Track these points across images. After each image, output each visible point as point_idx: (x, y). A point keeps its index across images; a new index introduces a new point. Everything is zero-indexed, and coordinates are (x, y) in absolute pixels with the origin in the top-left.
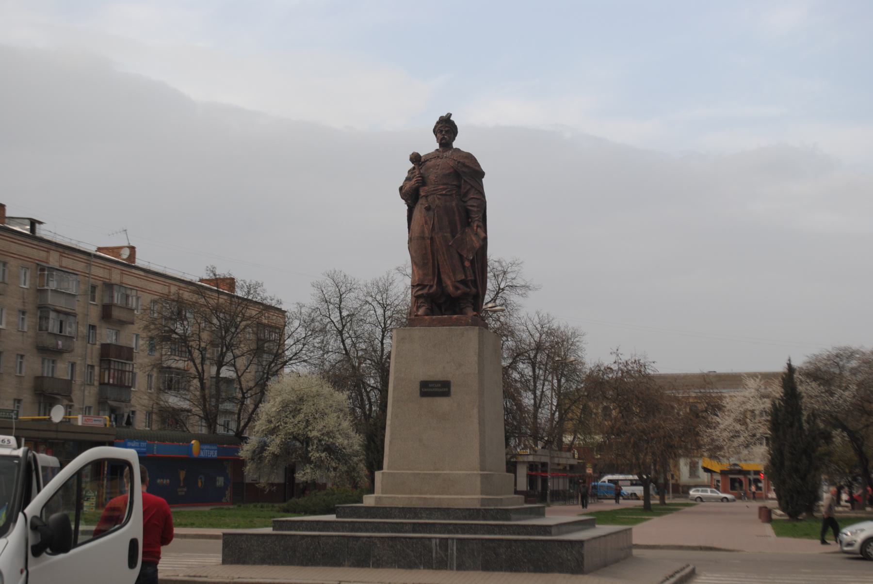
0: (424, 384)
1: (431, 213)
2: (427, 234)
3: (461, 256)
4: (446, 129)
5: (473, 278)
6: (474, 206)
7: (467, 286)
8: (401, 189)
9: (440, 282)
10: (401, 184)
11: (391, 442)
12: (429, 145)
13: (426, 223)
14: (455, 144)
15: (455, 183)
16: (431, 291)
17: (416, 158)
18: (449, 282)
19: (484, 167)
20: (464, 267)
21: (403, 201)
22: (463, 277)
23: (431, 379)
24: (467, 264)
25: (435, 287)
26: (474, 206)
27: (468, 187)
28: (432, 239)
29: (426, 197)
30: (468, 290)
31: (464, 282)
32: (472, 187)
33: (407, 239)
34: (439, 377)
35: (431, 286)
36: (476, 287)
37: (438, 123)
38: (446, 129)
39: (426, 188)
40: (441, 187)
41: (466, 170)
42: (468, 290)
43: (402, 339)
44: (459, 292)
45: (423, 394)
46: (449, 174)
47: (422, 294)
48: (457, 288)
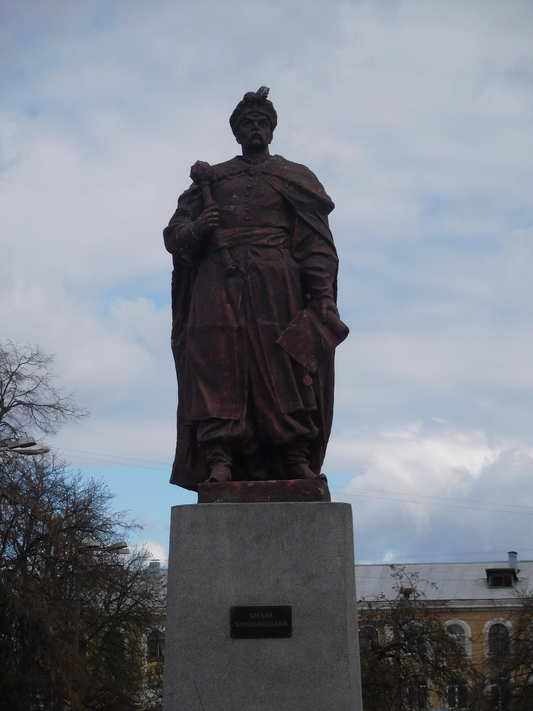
4: (254, 117)
5: (316, 407)
7: (306, 424)
8: (168, 233)
10: (166, 225)
12: (224, 148)
14: (273, 149)
15: (283, 224)
16: (236, 432)
19: (331, 191)
20: (301, 385)
22: (302, 406)
23: (254, 604)
24: (308, 380)
30: (306, 430)
34: (268, 600)
36: (319, 424)
38: (254, 117)
39: (228, 232)
42: (306, 430)
45: (238, 633)
47: (220, 438)
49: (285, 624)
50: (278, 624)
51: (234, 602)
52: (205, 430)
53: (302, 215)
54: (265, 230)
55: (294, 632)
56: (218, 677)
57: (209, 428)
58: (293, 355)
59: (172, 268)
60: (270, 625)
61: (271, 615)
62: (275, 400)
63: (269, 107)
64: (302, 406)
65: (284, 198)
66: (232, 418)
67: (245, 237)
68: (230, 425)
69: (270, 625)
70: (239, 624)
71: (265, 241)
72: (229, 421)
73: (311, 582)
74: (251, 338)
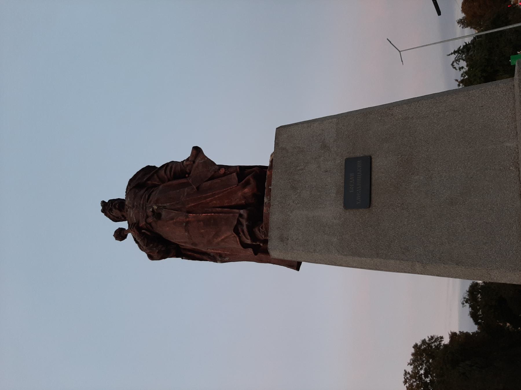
1: (164, 213)
3: (212, 178)
6: (171, 168)
8: (151, 257)
9: (239, 207)
13: (172, 219)
17: (120, 235)
18: (240, 194)
22: (235, 174)
23: (342, 189)
25: (242, 211)
26: (171, 168)
27: (155, 176)
28: (189, 212)
33: (212, 263)
34: (339, 178)
35: (241, 215)
37: (106, 215)
43: (282, 240)
44: (252, 181)
45: (368, 203)
47: (248, 226)
48: (247, 183)
55: (367, 154)
56: (406, 220)
57: (242, 233)
59: (180, 259)
62: (229, 190)
63: (112, 201)
64: (235, 174)
65: (134, 187)
67: (143, 208)
68: (241, 219)
71: (147, 196)
74: (193, 204)
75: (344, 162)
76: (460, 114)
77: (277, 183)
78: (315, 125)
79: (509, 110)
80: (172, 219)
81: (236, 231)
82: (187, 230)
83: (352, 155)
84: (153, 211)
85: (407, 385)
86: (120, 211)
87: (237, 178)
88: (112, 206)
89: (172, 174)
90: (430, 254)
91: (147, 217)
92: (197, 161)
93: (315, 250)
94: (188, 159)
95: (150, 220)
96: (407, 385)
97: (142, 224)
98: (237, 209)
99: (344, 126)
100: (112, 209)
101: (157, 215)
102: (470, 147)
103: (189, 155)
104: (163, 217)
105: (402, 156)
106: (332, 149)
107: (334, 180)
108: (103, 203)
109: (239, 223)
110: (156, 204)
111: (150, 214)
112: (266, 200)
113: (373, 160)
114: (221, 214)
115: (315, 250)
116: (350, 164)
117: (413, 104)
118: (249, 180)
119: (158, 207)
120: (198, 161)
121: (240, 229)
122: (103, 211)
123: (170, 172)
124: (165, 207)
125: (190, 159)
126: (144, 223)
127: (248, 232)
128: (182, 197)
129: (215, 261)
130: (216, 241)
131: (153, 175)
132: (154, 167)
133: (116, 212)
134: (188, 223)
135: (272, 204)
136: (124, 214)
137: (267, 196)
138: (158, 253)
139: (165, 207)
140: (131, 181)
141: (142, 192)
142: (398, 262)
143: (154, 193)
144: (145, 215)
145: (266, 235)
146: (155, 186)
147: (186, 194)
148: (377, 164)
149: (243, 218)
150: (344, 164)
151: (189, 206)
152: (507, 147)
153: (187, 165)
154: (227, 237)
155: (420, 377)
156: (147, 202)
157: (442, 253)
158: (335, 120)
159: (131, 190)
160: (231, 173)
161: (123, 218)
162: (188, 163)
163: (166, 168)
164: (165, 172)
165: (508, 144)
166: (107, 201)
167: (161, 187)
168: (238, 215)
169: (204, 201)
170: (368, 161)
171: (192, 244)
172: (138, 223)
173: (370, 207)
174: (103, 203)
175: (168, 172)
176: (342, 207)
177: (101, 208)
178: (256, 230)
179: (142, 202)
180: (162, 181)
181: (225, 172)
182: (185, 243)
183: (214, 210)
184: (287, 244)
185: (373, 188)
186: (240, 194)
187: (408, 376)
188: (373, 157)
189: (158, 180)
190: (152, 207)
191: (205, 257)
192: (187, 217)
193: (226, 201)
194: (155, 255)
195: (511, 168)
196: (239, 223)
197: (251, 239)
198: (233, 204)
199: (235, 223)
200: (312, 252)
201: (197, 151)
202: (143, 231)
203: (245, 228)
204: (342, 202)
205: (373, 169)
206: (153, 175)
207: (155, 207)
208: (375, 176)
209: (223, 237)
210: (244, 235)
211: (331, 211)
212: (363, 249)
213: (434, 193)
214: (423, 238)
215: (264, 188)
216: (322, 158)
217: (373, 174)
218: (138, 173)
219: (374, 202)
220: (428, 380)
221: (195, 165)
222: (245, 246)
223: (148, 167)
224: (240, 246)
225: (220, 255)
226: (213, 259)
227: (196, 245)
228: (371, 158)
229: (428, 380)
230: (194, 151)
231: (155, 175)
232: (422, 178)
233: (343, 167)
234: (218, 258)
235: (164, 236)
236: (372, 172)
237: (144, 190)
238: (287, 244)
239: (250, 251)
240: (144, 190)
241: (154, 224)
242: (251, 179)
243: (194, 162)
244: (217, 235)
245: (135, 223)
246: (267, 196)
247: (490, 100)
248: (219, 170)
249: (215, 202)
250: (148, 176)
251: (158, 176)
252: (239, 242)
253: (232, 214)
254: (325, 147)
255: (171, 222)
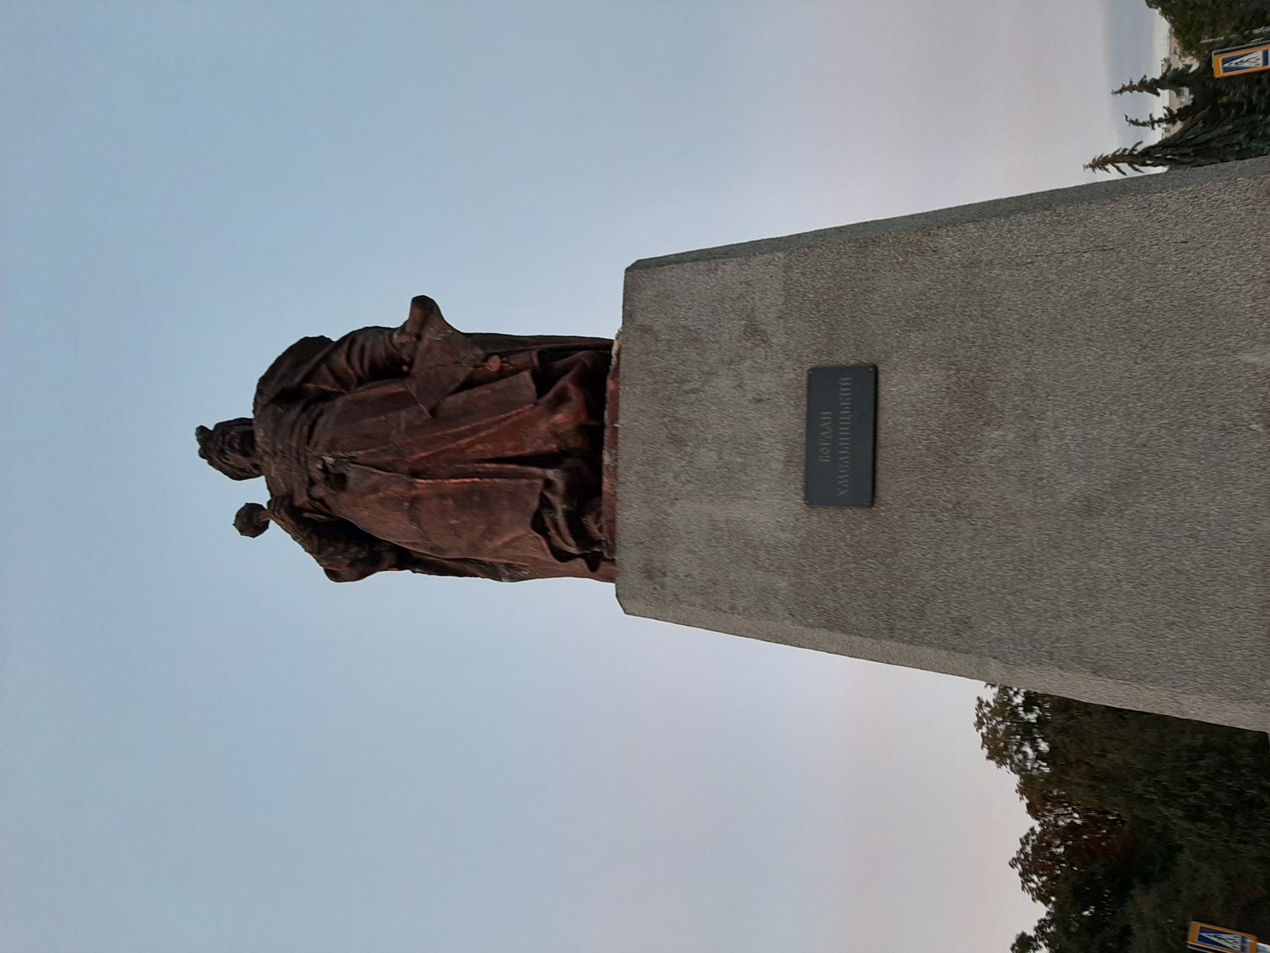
0: (817, 491)
1: (352, 474)
2: (398, 489)
3: (469, 384)
6: (362, 349)
8: (334, 575)
11: (1097, 670)
13: (375, 490)
16: (560, 485)
18: (543, 426)
20: (502, 374)
21: (379, 576)
22: (526, 374)
23: (801, 452)
24: (494, 364)
25: (550, 473)
26: (362, 349)
28: (415, 474)
29: (312, 483)
31: (543, 380)
32: (327, 358)
35: (548, 484)
37: (211, 463)
40: (295, 437)
41: (279, 374)
44: (573, 391)
46: (277, 420)
47: (568, 515)
48: (561, 399)
49: (845, 381)
50: (845, 397)
51: (796, 501)
52: (558, 538)
53: (298, 379)
54: (297, 429)
55: (865, 358)
56: (967, 546)
58: (453, 387)
59: (409, 572)
60: (846, 415)
61: (826, 415)
62: (516, 418)
63: (223, 427)
65: (272, 401)
66: (538, 491)
69: (846, 415)
70: (844, 488)
72: (543, 498)
73: (763, 327)
74: (423, 454)
75: (805, 377)
76: (1122, 262)
77: (633, 412)
78: (728, 268)
79: (1258, 259)
80: (375, 490)
81: (539, 525)
82: (415, 519)
83: (826, 361)
84: (325, 469)
85: (984, 730)
86: (246, 454)
87: (533, 386)
88: (223, 442)
89: (366, 364)
90: (1026, 641)
91: (312, 483)
92: (427, 336)
93: (733, 608)
94: (402, 329)
95: (319, 491)
96: (984, 730)
97: (301, 500)
98: (538, 466)
99: (804, 274)
100: (225, 446)
101: (338, 481)
102: (1145, 359)
103: (407, 318)
104: (351, 483)
105: (958, 371)
106: (774, 340)
107: (779, 425)
108: (202, 431)
109: (545, 503)
110: (329, 451)
111: (318, 476)
112: (607, 459)
113: (882, 377)
114: (497, 480)
115: (733, 608)
116: (821, 381)
117: (993, 223)
118: (564, 389)
119: (337, 458)
120: (430, 335)
121: (547, 520)
122: (204, 454)
123: (361, 360)
124: (352, 460)
125: (408, 329)
126: (306, 498)
127: (571, 527)
128: (394, 432)
129: (497, 576)
130: (490, 545)
131: (317, 367)
132: (322, 341)
133: (236, 459)
134: (415, 500)
135: (621, 479)
136: (258, 462)
137: (611, 447)
138: (350, 565)
139: (352, 460)
140: (263, 382)
141: (294, 413)
142: (944, 653)
143: (322, 420)
144: (306, 479)
145: (612, 535)
146: (326, 397)
147: (403, 426)
148: (893, 388)
149: (554, 493)
150: (804, 383)
151: (415, 457)
152: (1246, 364)
153: (403, 345)
154: (515, 539)
155: (1014, 713)
156: (308, 444)
157: (1058, 639)
158: (781, 255)
159: (264, 407)
160: (517, 371)
161: (256, 472)
162: (404, 339)
163: (350, 348)
164: (348, 359)
165: (1252, 359)
166: (211, 428)
167: (339, 403)
168: (540, 482)
169: (452, 446)
170: (869, 377)
171: (432, 549)
172: (290, 496)
173: (872, 504)
174: (202, 431)
175: (356, 363)
176: (799, 499)
177: (198, 446)
178: (589, 521)
179: (294, 444)
180: (343, 382)
181: (501, 368)
182: (414, 544)
183: (481, 467)
184: (663, 587)
185: (881, 454)
186: (543, 426)
187: (986, 710)
188: (881, 368)
189: (331, 379)
190: (320, 458)
191: (469, 568)
192: (412, 486)
193: (508, 445)
194: (344, 570)
195: (1254, 426)
196: (545, 503)
197: (578, 545)
198: (528, 451)
199: (535, 503)
200: (725, 612)
201: (424, 307)
202: (306, 515)
203: (562, 522)
204: (799, 485)
205: (882, 403)
206: (317, 367)
207: (330, 460)
208: (886, 421)
209: (506, 539)
210: (559, 534)
211: (771, 506)
212: (855, 614)
213: (1041, 479)
214: (1009, 597)
215: (603, 426)
216: (748, 363)
217: (883, 417)
218: (280, 360)
219: (881, 493)
220: (1032, 717)
221: (423, 346)
222: (562, 556)
223: (306, 341)
224: (551, 559)
225: (508, 566)
226: (493, 572)
227: (442, 551)
228: (875, 368)
229: (1032, 717)
230: (418, 311)
231: (324, 369)
232: (1010, 437)
233: (802, 392)
234: (503, 569)
235: (361, 526)
236: (880, 412)
237: (298, 408)
238: (663, 587)
239: (580, 563)
240: (298, 408)
241: (330, 501)
242: (571, 387)
243: (419, 337)
244: (491, 532)
245: (284, 498)
246: (611, 447)
247: (1209, 225)
248: (486, 360)
249: (480, 447)
250: (306, 368)
251: (330, 369)
252: (548, 552)
253: (525, 481)
254: (753, 331)
255: (372, 497)
